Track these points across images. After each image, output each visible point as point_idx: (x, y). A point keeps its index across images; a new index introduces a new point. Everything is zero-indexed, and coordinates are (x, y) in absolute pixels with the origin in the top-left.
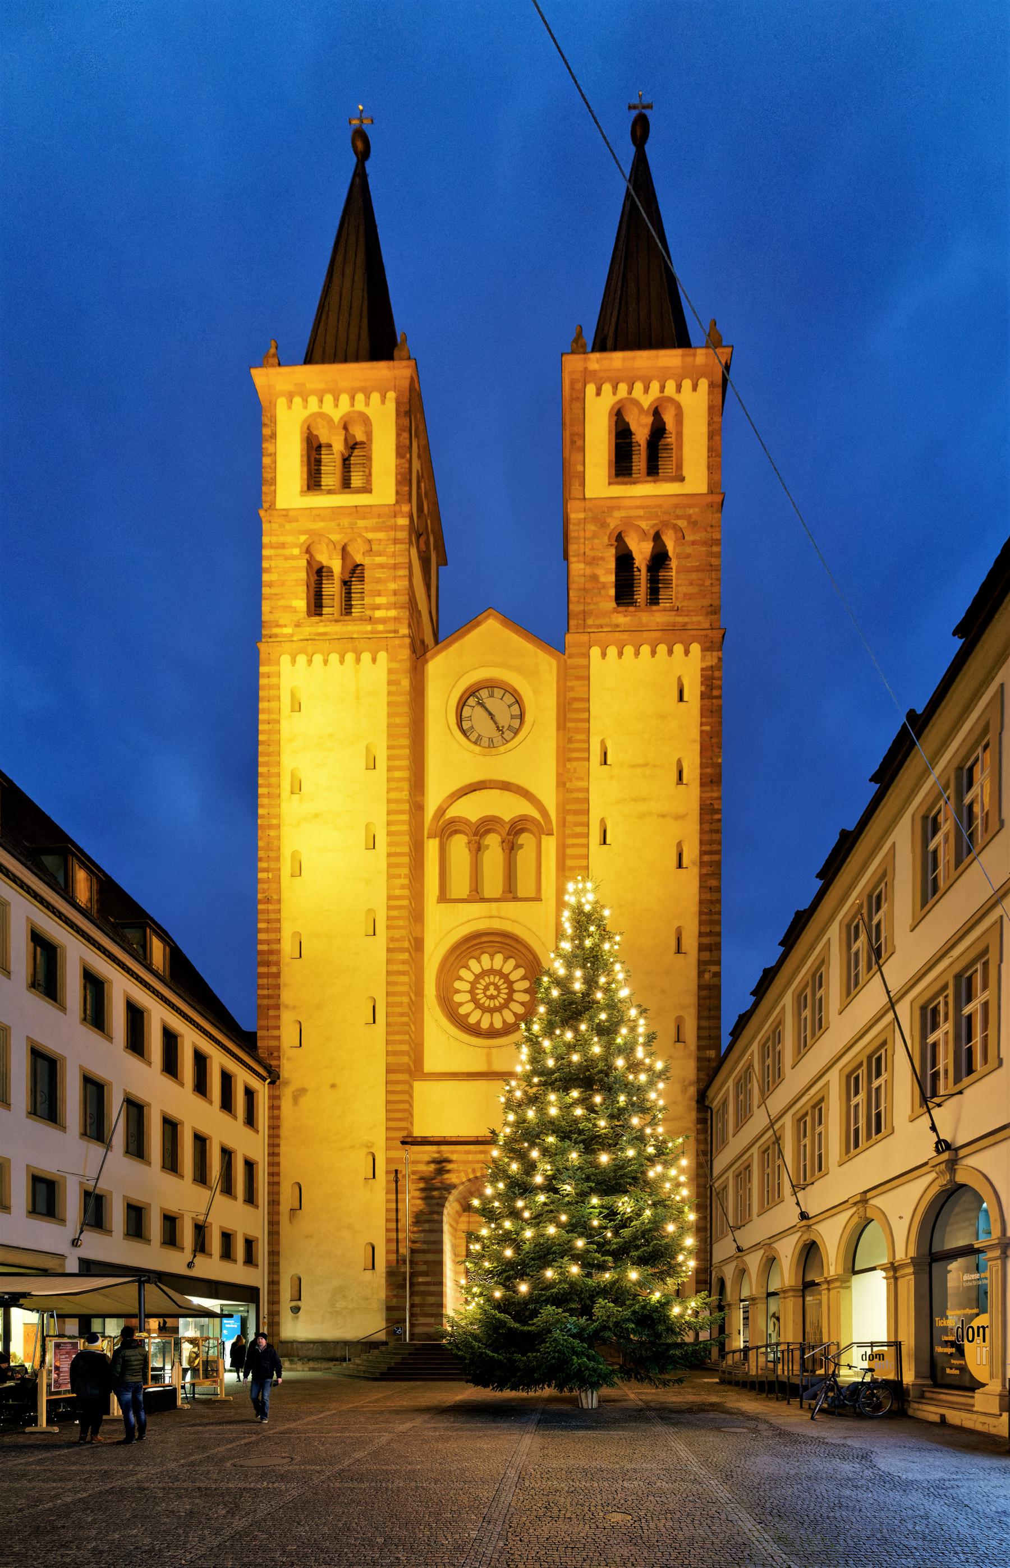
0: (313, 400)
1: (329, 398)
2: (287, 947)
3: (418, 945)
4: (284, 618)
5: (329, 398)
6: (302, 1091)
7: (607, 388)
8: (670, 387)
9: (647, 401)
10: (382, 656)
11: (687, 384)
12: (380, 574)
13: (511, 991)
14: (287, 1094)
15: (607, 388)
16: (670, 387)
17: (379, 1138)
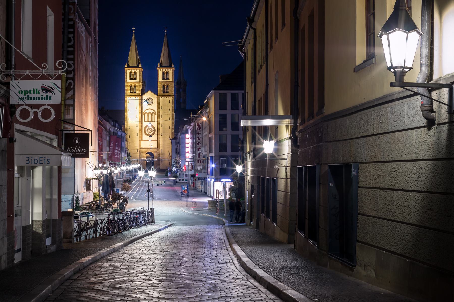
0: (131, 70)
1: (132, 70)
2: (128, 127)
3: (142, 126)
4: (128, 93)
5: (132, 70)
6: (130, 143)
7: (162, 70)
8: (168, 70)
9: (166, 72)
10: (138, 97)
11: (170, 70)
12: (138, 89)
13: (152, 130)
14: (128, 143)
15: (162, 70)
16: (168, 70)
17: (138, 148)
